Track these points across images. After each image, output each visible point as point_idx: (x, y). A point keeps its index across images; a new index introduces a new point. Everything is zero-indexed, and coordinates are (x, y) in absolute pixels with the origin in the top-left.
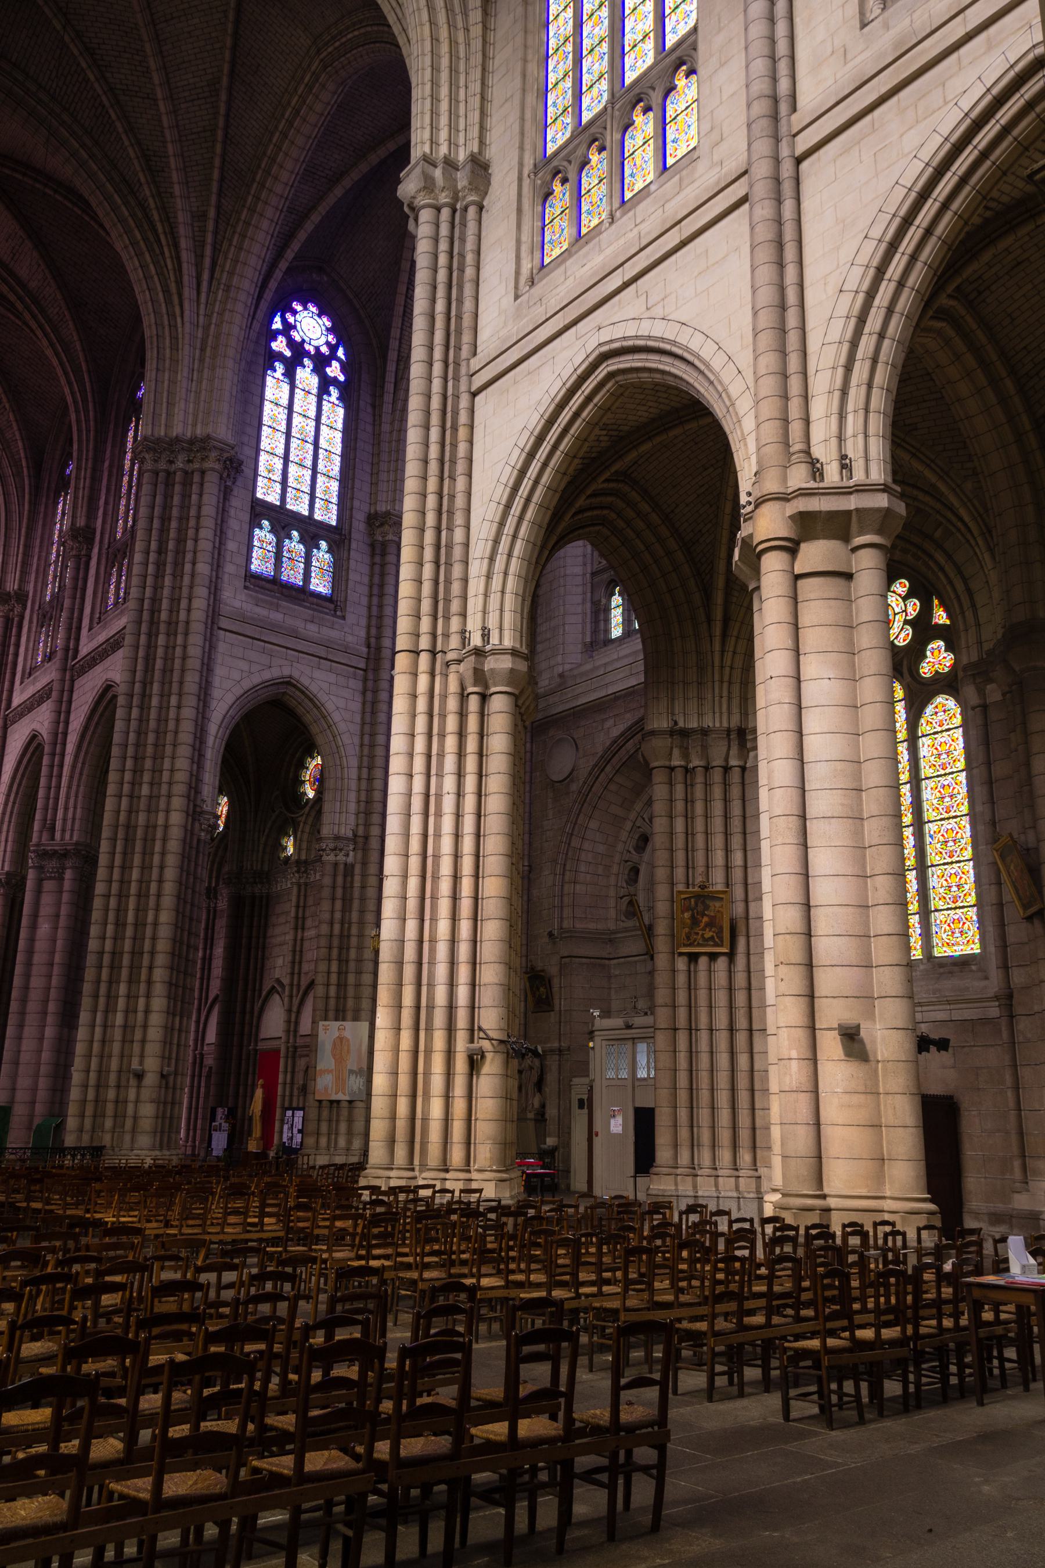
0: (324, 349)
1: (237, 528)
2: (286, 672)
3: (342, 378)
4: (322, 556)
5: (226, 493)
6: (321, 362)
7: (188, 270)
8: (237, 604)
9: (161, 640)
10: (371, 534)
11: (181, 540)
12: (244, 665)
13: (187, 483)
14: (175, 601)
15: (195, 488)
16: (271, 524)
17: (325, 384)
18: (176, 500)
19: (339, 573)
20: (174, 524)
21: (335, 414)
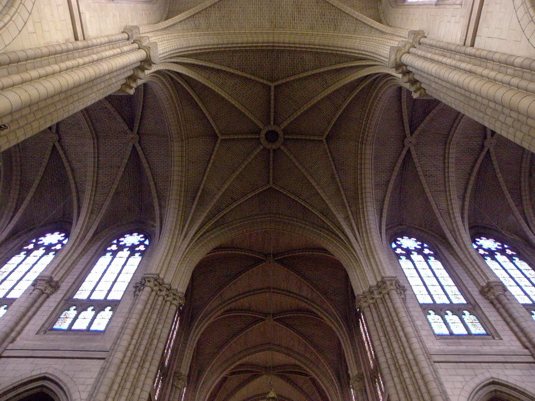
0: (420, 247)
1: (418, 315)
2: (488, 375)
3: (432, 253)
4: (468, 317)
5: (404, 300)
6: (420, 251)
7: (353, 240)
8: (437, 348)
9: (406, 375)
10: (487, 298)
11: (392, 324)
12: (460, 379)
14: (403, 353)
15: (388, 301)
16: (434, 311)
17: (426, 257)
18: (382, 310)
19: (483, 320)
20: (386, 320)
21: (436, 264)
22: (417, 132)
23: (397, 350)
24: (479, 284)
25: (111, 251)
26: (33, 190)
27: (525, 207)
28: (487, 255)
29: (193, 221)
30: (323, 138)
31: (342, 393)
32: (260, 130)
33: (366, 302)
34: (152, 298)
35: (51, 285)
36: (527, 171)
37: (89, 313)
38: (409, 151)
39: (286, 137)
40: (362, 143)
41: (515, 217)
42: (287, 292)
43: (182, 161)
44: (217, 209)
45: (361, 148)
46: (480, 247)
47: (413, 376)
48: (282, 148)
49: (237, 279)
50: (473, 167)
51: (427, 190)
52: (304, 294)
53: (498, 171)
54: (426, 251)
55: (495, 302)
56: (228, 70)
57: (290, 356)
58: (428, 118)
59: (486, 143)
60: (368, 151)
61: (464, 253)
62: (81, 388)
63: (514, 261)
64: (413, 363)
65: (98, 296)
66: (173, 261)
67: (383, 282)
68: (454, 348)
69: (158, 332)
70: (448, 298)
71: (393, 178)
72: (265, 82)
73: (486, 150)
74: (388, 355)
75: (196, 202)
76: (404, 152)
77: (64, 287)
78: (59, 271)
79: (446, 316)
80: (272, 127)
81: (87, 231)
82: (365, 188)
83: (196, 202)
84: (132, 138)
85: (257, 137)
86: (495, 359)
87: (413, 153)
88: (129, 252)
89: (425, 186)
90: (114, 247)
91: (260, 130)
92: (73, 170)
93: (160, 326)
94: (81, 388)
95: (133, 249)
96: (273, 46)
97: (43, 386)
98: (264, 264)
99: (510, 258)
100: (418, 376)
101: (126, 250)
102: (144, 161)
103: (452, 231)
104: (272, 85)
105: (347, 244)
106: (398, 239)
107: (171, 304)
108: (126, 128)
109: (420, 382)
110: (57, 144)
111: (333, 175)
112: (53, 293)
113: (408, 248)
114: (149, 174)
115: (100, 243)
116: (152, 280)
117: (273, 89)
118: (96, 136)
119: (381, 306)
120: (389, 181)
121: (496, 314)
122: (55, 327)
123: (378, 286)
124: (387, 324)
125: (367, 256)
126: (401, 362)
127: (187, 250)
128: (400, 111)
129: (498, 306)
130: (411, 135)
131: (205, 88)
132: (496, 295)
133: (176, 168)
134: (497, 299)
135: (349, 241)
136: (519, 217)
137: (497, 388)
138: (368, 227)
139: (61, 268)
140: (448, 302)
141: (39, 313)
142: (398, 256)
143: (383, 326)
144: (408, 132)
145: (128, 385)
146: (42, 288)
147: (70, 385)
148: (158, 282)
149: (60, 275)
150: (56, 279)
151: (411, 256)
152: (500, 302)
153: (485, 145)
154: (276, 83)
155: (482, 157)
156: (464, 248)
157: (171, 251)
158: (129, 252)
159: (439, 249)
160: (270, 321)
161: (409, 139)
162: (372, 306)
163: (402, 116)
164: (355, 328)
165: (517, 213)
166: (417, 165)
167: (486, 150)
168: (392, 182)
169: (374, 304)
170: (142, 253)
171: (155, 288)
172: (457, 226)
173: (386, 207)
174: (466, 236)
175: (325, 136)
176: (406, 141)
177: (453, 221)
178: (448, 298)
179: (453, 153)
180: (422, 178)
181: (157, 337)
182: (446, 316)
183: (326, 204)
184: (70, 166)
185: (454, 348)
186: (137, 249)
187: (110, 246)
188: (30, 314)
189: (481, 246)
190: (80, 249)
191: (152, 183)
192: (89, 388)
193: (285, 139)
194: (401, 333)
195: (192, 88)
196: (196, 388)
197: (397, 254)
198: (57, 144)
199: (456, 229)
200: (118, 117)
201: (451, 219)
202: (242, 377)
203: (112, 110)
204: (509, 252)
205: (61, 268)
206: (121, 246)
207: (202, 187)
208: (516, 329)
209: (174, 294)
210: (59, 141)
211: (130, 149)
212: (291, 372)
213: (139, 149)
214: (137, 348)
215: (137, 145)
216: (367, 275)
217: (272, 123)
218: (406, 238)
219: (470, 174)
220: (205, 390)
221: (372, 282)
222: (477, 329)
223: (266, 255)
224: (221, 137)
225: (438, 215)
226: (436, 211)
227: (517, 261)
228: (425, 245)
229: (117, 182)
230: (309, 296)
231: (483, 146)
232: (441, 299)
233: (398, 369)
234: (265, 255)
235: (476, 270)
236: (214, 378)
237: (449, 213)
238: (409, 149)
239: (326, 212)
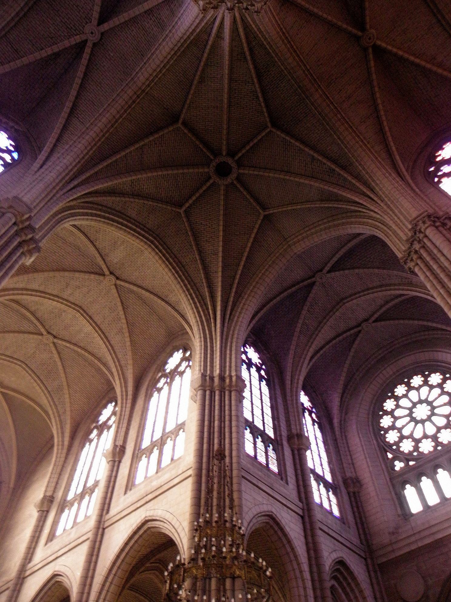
22: (78, 39)
30: (179, 125)
38: (101, 22)
80: (215, 178)
87: (96, 15)
108: (315, 288)
117: (184, 208)
130: (86, 41)
144: (88, 50)
161: (92, 39)
176: (95, 38)
200: (309, 299)
203: (306, 308)
210: (366, 320)
213: (327, 268)
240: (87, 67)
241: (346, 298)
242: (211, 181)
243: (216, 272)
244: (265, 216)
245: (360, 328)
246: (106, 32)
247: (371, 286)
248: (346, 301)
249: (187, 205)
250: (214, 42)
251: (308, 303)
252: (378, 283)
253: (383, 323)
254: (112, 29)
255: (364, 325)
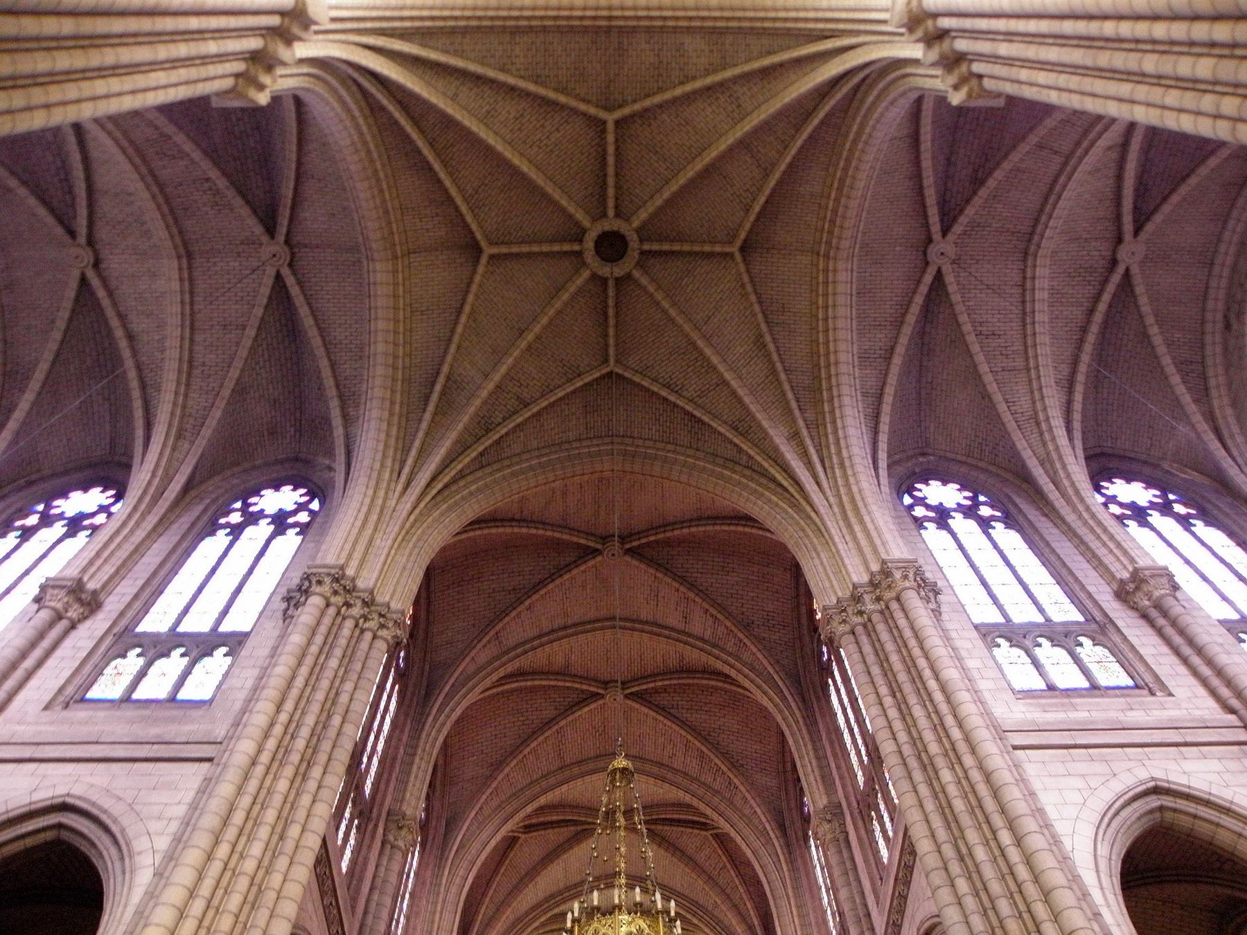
0: (968, 503)
1: (970, 646)
2: (1143, 774)
3: (998, 514)
4: (1089, 651)
5: (937, 613)
6: (969, 511)
8: (1019, 716)
9: (946, 776)
10: (1134, 608)
13: (886, 614)
14: (940, 727)
15: (898, 615)
17: (985, 524)
18: (885, 636)
19: (1126, 656)
20: (894, 658)
21: (1008, 538)
22: (957, 229)
23: (923, 723)
24: (1113, 577)
25: (228, 525)
26: (35, 384)
27: (1216, 403)
28: (1129, 517)
29: (423, 453)
30: (734, 249)
31: (791, 862)
32: (584, 231)
33: (844, 621)
34: (327, 621)
35: (79, 600)
36: (1219, 316)
37: (175, 663)
38: (939, 275)
39: (646, 247)
40: (827, 256)
41: (1193, 426)
42: (656, 627)
43: (396, 309)
44: (484, 425)
45: (826, 270)
46: (1112, 499)
47: (964, 780)
48: (636, 274)
49: (535, 597)
50: (1091, 311)
51: (984, 368)
52: (696, 629)
53: (1150, 320)
54: (985, 511)
55: (1154, 613)
56: (502, 77)
57: (664, 780)
58: (983, 192)
59: (1123, 253)
60: (842, 276)
61: (1075, 509)
62: (154, 826)
63: (1193, 528)
64: (962, 747)
65: (198, 623)
66: (379, 541)
67: (886, 572)
68: (1061, 716)
69: (344, 698)
70: (1041, 610)
71: (904, 340)
72: (592, 110)
73: (1121, 270)
74: (902, 737)
75: (431, 408)
76: (928, 278)
77: (113, 605)
78: (99, 569)
79: (1037, 651)
81: (168, 479)
82: (837, 363)
83: (431, 408)
84: (274, 256)
85: (576, 247)
86: (1157, 737)
87: (949, 279)
88: (272, 527)
89: (980, 358)
90: (235, 518)
91: (584, 231)
92: (131, 337)
93: (349, 686)
94: (154, 826)
95: (281, 522)
96: (610, 18)
97: (60, 826)
98: (599, 558)
99: (1184, 521)
100: (975, 775)
101: (263, 522)
102: (304, 311)
103: (1046, 462)
104: (611, 118)
105: (796, 497)
106: (918, 486)
107: (375, 637)
108: (259, 230)
109: (982, 789)
110: (90, 274)
111: (761, 336)
112: (86, 618)
113: (941, 504)
114: (316, 341)
115: (201, 507)
116: (328, 580)
117: (610, 126)
118: (187, 253)
119: (881, 628)
120: (892, 349)
121: (1156, 640)
122: (89, 695)
123: (873, 584)
124: (898, 666)
125: (846, 518)
126: (934, 748)
127: (412, 518)
128: (918, 176)
129: (1161, 621)
130: (944, 235)
131: (449, 122)
132: (1154, 597)
133: (381, 325)
134: (1158, 606)
135: (801, 489)
136: (1203, 427)
137: (1165, 803)
138: (845, 454)
139: (106, 561)
140: (1041, 619)
141: (51, 662)
142: (919, 523)
143: (888, 672)
144: (936, 228)
145: (270, 815)
146: (59, 606)
147: (125, 821)
148: (342, 583)
149: (103, 576)
150: (92, 585)
151: (950, 521)
152: (1165, 614)
153: (1119, 257)
154: (618, 114)
155: (1111, 288)
156: (1074, 498)
157: (374, 517)
158: (272, 527)
159: (1016, 505)
160: (615, 700)
162: (859, 630)
163: (921, 188)
164: (818, 699)
165: (1197, 418)
166: (959, 308)
167: (1121, 270)
168: (900, 350)
169: (865, 626)
170: (304, 529)
171: (333, 600)
172: (1057, 448)
173: (886, 408)
174: (1079, 473)
175: (739, 243)
176: (933, 251)
177: (1047, 436)
178: (1041, 610)
179: (1043, 272)
180: (971, 338)
181: (340, 709)
182: (1037, 651)
183: (745, 407)
184: (124, 326)
185: (1061, 716)
186: (291, 520)
187: (227, 514)
188: (28, 663)
189: (1115, 497)
190: (152, 520)
191: (324, 364)
192: (174, 827)
193: (642, 253)
194: (932, 684)
195: (416, 122)
196: (442, 858)
197: (916, 519)
198: (90, 274)
199: (1055, 456)
200: (238, 202)
201: (1041, 434)
202: (554, 836)
203: (222, 183)
204: (1179, 509)
205: (106, 561)
206: (252, 514)
207: (445, 369)
208: (1206, 671)
209: (381, 615)
210: (96, 265)
211: (269, 281)
212: (671, 822)
213: (290, 280)
214: (291, 730)
215: (286, 271)
216: (847, 561)
217: (611, 213)
218: (935, 484)
219: (1084, 330)
220: (465, 864)
221: (859, 576)
222: (1112, 674)
223: (605, 539)
224: (489, 250)
225: (1011, 425)
226: (1007, 418)
227: (1199, 527)
228: (982, 498)
229: (238, 364)
230: (708, 635)
231: (1114, 262)
232: (1023, 613)
233: (929, 767)
234: (601, 538)
235: (1104, 544)
236: (484, 835)
237: (1037, 421)
238: (939, 271)
239: (746, 426)
240: (924, 206)
241: (190, 268)
242: (611, 213)
243: (454, 98)
244: (480, 251)
245: (82, 239)
246: (924, 271)
247: (199, 338)
248: (185, 265)
249: (611, 138)
250: (794, 421)
251: (231, 193)
252: (199, 358)
253: (71, 293)
254: (919, 282)
255: (88, 257)
